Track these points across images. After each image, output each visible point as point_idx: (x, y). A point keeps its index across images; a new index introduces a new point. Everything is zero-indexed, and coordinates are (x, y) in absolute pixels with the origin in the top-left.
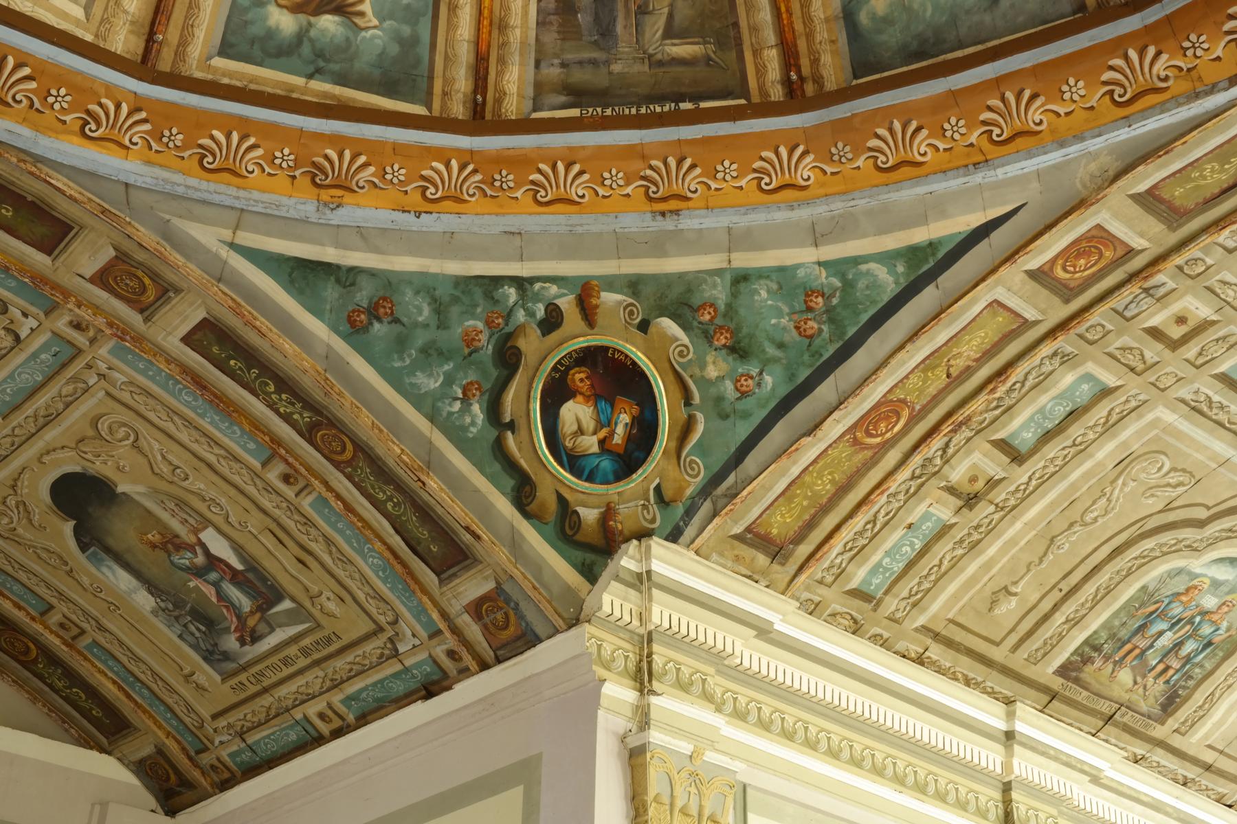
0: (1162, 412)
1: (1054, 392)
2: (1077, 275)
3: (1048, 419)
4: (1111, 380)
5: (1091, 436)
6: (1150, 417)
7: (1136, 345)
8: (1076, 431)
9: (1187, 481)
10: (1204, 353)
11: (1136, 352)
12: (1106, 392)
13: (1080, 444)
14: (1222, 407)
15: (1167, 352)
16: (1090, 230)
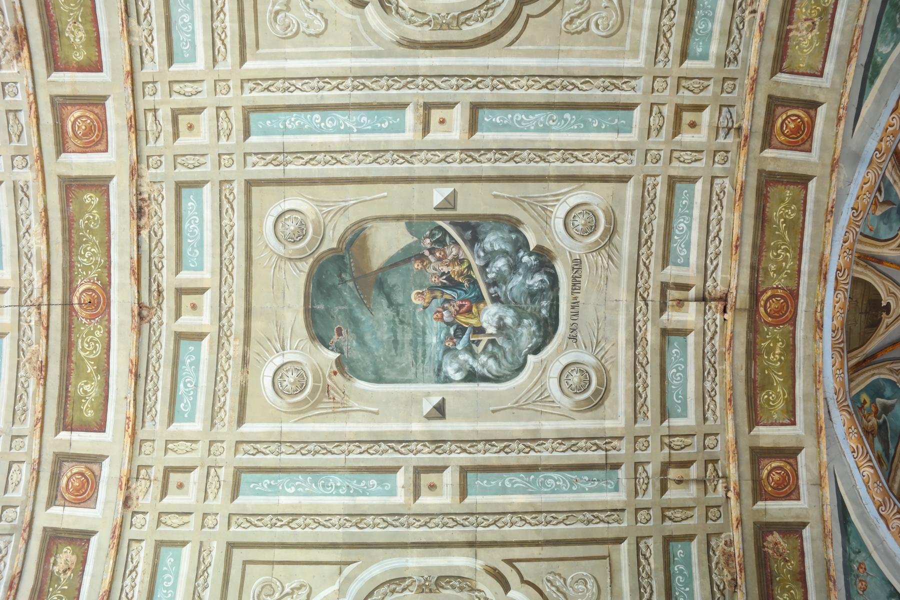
0: (640, 63)
1: (716, 35)
2: (784, 116)
3: (703, 16)
4: (688, 64)
5: (665, 21)
6: (642, 55)
7: (701, 94)
8: (680, 19)
9: (568, 26)
10: (659, 115)
11: (696, 91)
12: (684, 55)
13: (668, 12)
14: (606, 88)
15: (679, 102)
16: (811, 146)
